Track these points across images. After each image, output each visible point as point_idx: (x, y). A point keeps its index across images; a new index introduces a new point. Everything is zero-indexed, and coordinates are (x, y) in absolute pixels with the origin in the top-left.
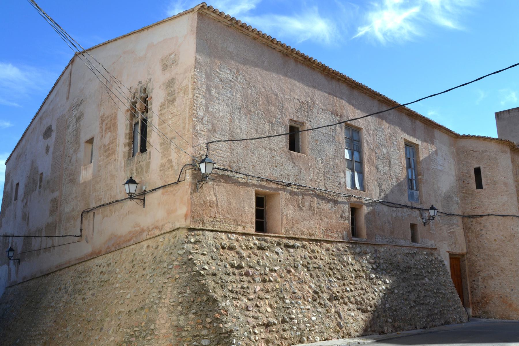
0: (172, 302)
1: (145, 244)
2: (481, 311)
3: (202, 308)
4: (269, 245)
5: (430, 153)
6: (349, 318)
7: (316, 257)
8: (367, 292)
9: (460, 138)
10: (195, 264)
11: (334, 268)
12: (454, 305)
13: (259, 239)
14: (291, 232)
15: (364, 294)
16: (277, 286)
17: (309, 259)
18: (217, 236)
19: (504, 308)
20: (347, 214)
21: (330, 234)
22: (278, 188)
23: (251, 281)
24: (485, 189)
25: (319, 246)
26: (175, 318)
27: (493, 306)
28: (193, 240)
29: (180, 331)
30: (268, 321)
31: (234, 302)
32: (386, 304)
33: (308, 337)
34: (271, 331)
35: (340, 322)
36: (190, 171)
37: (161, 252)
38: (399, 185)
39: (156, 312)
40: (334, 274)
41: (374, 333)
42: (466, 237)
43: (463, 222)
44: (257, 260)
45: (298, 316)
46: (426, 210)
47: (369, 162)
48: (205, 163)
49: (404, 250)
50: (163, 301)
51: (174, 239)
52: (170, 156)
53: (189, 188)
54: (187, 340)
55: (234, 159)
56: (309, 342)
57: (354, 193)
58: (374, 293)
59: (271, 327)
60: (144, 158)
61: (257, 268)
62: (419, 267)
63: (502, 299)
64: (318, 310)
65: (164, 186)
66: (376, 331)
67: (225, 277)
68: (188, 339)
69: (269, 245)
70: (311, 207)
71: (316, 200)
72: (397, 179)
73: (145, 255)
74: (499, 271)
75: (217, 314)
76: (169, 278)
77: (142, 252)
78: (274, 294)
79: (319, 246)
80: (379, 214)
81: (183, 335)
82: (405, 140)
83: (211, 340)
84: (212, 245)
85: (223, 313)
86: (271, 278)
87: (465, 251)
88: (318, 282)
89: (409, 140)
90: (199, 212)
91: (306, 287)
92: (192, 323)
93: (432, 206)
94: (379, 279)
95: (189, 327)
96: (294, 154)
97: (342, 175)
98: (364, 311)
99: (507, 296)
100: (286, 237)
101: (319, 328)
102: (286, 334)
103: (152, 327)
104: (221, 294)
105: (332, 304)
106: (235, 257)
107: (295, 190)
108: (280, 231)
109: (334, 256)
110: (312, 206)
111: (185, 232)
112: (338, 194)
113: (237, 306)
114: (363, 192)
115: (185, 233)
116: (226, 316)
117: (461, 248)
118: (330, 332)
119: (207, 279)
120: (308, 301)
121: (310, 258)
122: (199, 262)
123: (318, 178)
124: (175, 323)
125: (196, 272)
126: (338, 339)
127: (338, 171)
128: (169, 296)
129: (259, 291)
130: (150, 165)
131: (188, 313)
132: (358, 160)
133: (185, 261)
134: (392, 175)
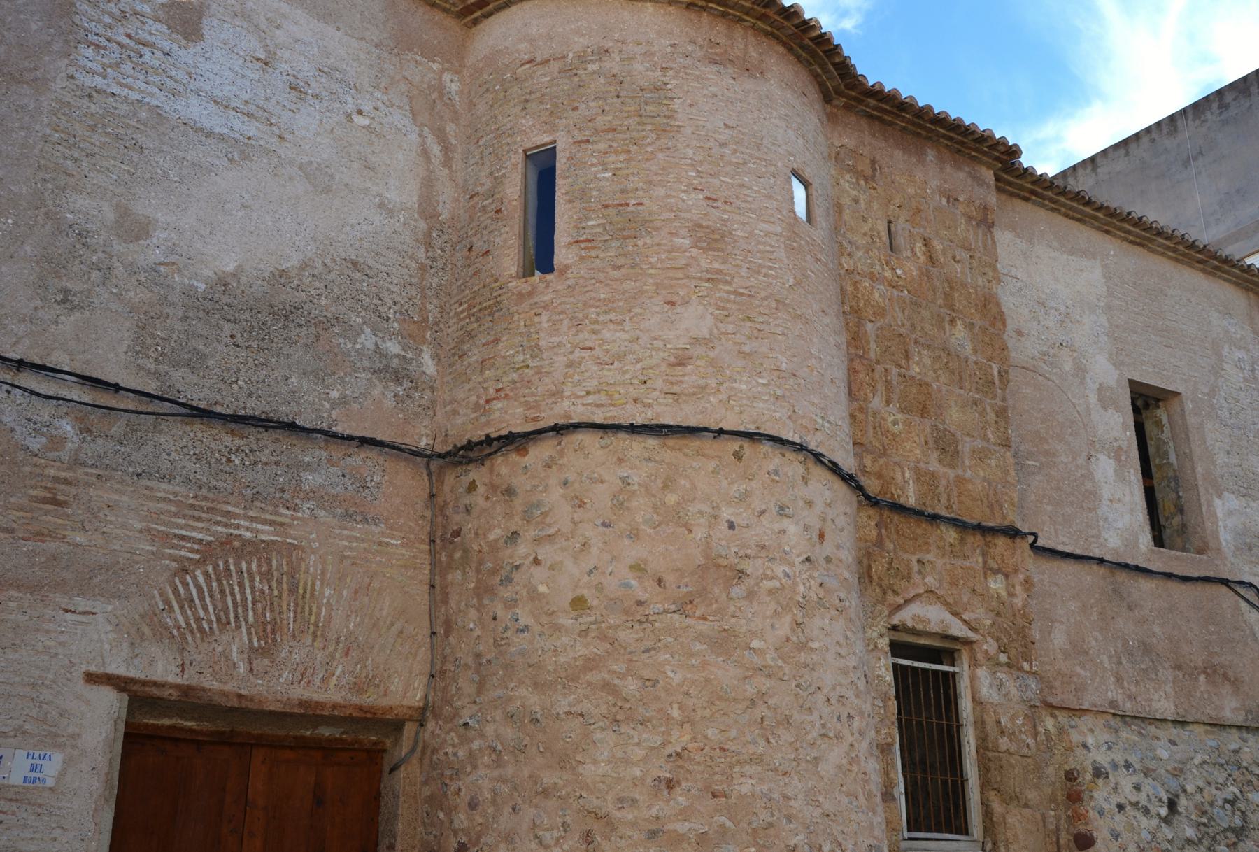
87: (416, 698)
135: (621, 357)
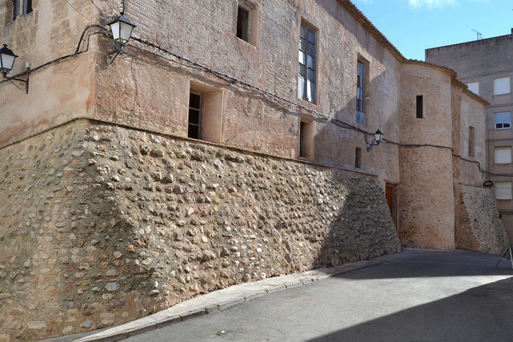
0: (59, 228)
1: (26, 144)
2: (407, 240)
3: (108, 237)
4: (206, 155)
5: (379, 73)
6: (298, 249)
7: (262, 175)
8: (315, 219)
9: (407, 63)
10: (99, 171)
11: (281, 189)
12: (391, 234)
13: (194, 146)
14: (233, 142)
15: (312, 222)
16: (216, 209)
17: (254, 177)
18: (135, 135)
19: (429, 238)
20: (297, 128)
21: (277, 150)
22: (221, 83)
23: (182, 200)
24: (425, 119)
25: (265, 162)
26: (64, 251)
27: (419, 235)
28: (97, 137)
29: (71, 271)
30: (204, 254)
31: (157, 228)
32: (333, 233)
33: (252, 274)
34: (207, 268)
35: (288, 255)
36: (96, 36)
37: (47, 153)
38: (350, 104)
39: (33, 242)
40: (282, 196)
41: (322, 266)
42: (401, 166)
43: (399, 151)
44: (190, 173)
45: (241, 248)
46: (371, 134)
47: (322, 71)
48: (118, 23)
49: (349, 175)
50: (45, 225)
51: (69, 135)
52: (67, 15)
53: (93, 63)
54: (83, 284)
55: (163, 32)
56: (253, 280)
57: (304, 104)
58: (321, 220)
59: (207, 262)
60: (28, 23)
61: (190, 183)
62: (363, 194)
63: (428, 230)
64: (265, 240)
65: (57, 61)
66: (324, 264)
67: (145, 194)
68: (85, 283)
69: (206, 155)
70: (258, 113)
71: (264, 105)
72: (348, 96)
73: (26, 159)
74: (429, 202)
75: (132, 246)
76: (56, 191)
77: (21, 155)
78: (212, 218)
79: (265, 162)
80: (328, 132)
81: (77, 277)
82: (359, 54)
83: (121, 284)
84: (127, 147)
85: (140, 244)
86: (208, 198)
87: (398, 181)
88: (264, 205)
89: (362, 55)
90: (109, 99)
91: (250, 211)
92: (92, 259)
93: (379, 130)
94: (327, 205)
95: (86, 265)
96: (242, 42)
97: (294, 80)
98: (313, 241)
99: (433, 227)
100: (228, 148)
101: (265, 261)
102: (227, 271)
103: (27, 264)
104: (139, 217)
105: (279, 232)
106: (160, 167)
107: (241, 90)
108: (220, 139)
109: (281, 175)
110: (259, 112)
111: (84, 124)
112: (289, 104)
113: (161, 234)
114: (314, 105)
115: (86, 126)
116: (145, 249)
117: (395, 179)
118: (277, 266)
119: (117, 195)
120: (253, 229)
121: (256, 175)
122: (105, 169)
123: (268, 79)
124: (64, 259)
125: (99, 183)
126: (286, 274)
127: (290, 75)
128: (55, 217)
129: (193, 214)
130: (37, 32)
131: (86, 243)
132: (311, 67)
133: (83, 166)
134: (343, 90)
135: (434, 134)
